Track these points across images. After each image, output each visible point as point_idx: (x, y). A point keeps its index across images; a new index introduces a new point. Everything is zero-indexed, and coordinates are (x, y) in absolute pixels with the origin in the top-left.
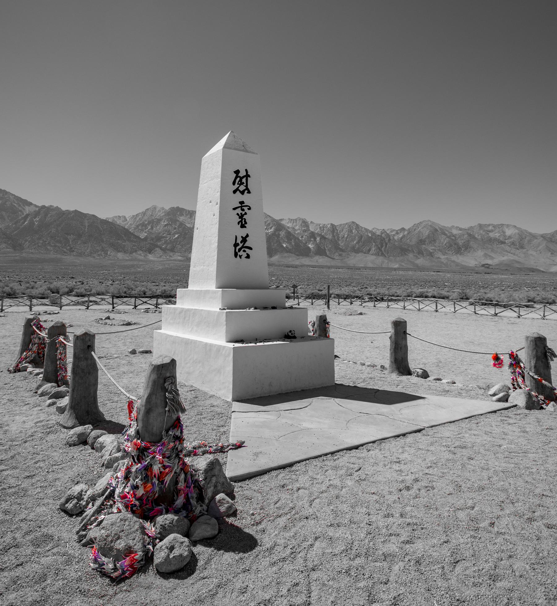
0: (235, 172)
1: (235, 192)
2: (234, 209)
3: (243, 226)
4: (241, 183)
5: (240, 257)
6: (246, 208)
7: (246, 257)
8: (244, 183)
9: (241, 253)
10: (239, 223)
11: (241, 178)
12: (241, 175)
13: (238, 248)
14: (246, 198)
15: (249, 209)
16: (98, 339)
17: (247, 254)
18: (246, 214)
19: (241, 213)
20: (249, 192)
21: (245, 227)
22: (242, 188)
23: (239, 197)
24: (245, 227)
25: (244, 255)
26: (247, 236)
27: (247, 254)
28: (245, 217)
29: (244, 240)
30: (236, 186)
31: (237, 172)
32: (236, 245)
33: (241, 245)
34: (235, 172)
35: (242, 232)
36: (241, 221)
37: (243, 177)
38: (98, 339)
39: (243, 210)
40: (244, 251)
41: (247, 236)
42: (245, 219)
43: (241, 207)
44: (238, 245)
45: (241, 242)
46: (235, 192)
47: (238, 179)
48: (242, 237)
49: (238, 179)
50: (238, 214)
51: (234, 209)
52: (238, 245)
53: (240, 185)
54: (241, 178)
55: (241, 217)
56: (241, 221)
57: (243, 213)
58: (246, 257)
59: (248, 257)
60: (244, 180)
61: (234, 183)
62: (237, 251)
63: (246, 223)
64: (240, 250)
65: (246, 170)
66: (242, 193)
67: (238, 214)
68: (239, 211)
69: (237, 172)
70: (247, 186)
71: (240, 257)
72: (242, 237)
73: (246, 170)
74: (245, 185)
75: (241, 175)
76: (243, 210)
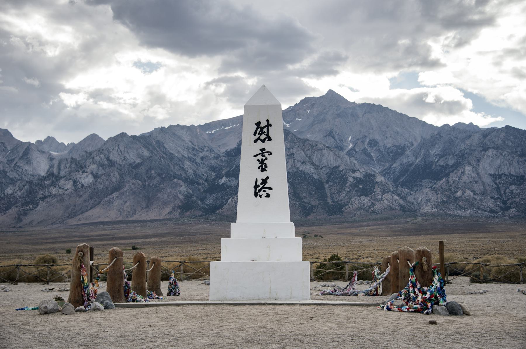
0: (256, 124)
1: (256, 141)
2: (255, 156)
3: (263, 170)
4: (262, 132)
5: (261, 196)
6: (266, 154)
7: (266, 197)
8: (265, 132)
9: (261, 193)
10: (259, 168)
12: (262, 125)
13: (258, 189)
14: (267, 145)
15: (270, 154)
17: (267, 194)
18: (266, 159)
19: (262, 159)
20: (270, 139)
21: (266, 171)
22: (263, 137)
24: (266, 171)
25: (265, 194)
26: (268, 178)
27: (267, 194)
28: (265, 162)
29: (264, 181)
30: (257, 136)
31: (258, 124)
32: (256, 186)
33: (261, 186)
34: (256, 124)
35: (264, 175)
36: (262, 166)
37: (264, 127)
39: (264, 156)
41: (268, 178)
42: (265, 164)
43: (262, 154)
44: (259, 186)
45: (261, 184)
46: (256, 141)
48: (262, 179)
49: (259, 130)
50: (258, 160)
51: (255, 156)
52: (259, 186)
53: (261, 135)
54: (262, 128)
55: (262, 162)
57: (264, 158)
58: (266, 197)
59: (268, 196)
60: (265, 130)
61: (255, 134)
62: (257, 191)
63: (266, 167)
64: (260, 191)
65: (268, 121)
67: (258, 160)
68: (260, 157)
71: (261, 196)
72: (262, 179)
73: (268, 121)
74: (266, 134)
75: (262, 125)
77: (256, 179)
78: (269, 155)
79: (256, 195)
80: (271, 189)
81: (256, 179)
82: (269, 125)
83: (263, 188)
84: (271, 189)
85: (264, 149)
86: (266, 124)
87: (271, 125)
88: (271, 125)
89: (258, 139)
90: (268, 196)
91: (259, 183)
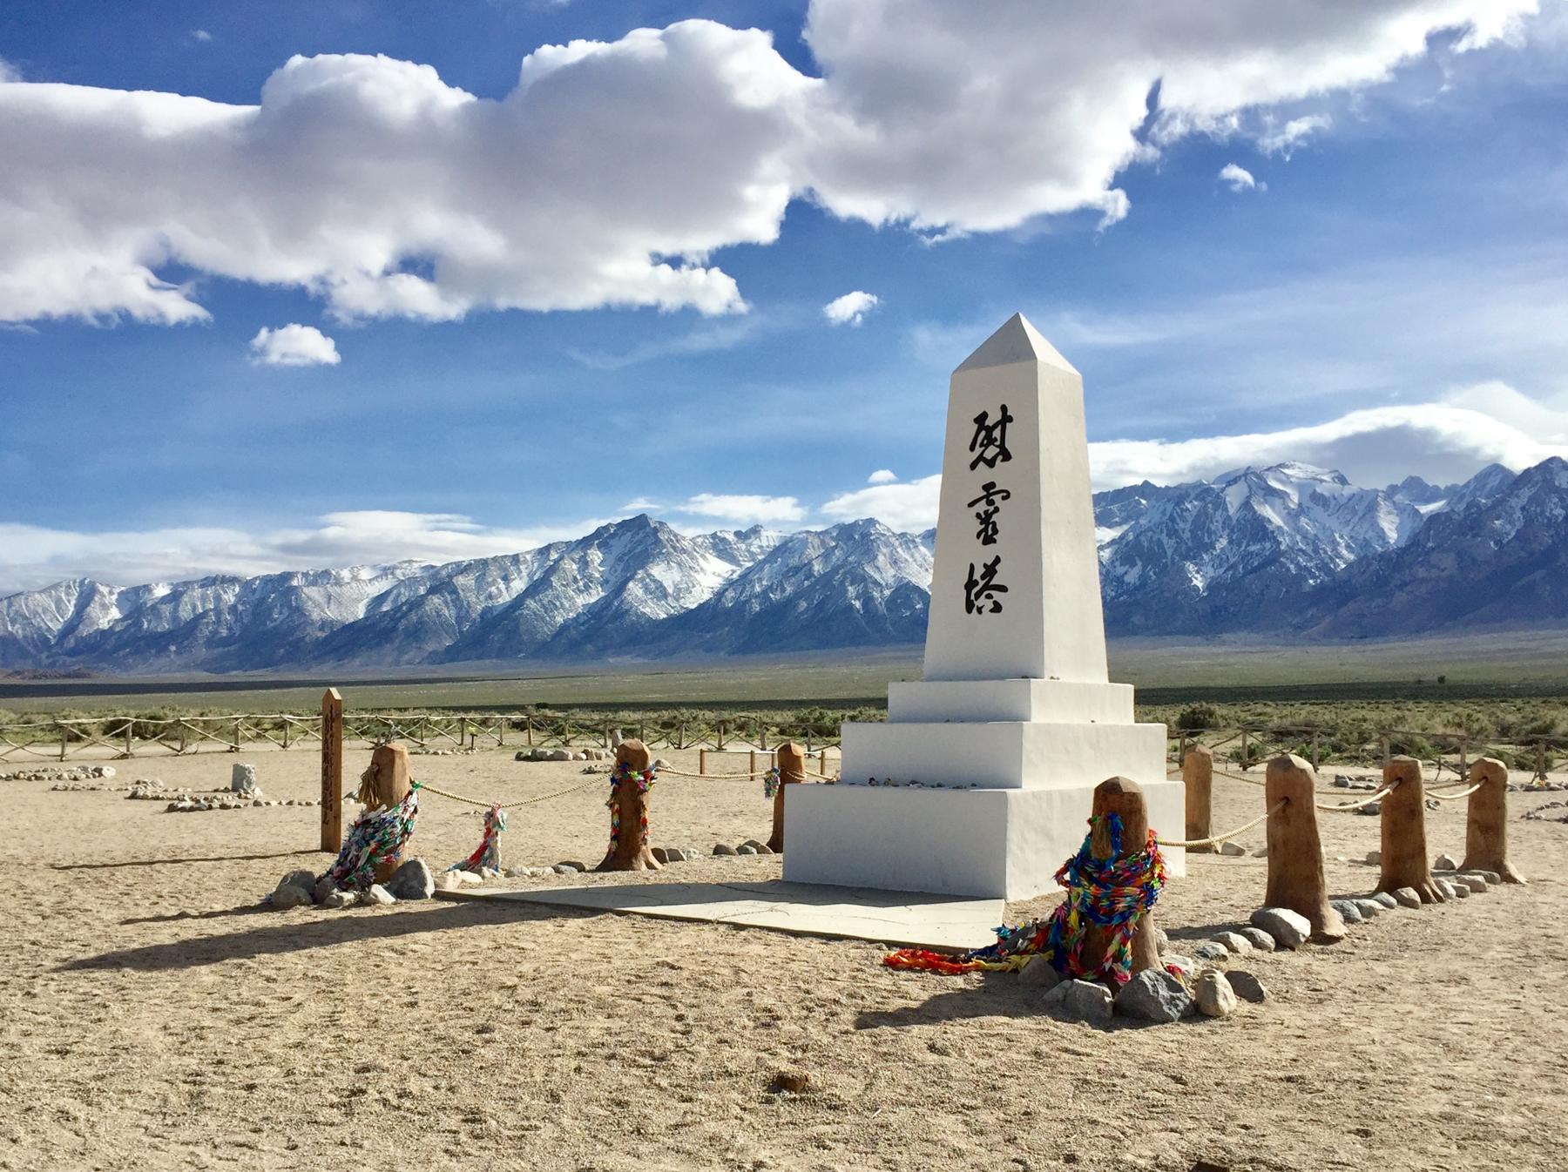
0: (976, 421)
1: (973, 466)
2: (971, 505)
3: (989, 540)
4: (990, 441)
5: (980, 610)
6: (997, 498)
9: (982, 601)
11: (990, 430)
12: (989, 422)
13: (974, 591)
14: (1001, 475)
16: (313, 823)
17: (996, 603)
18: (997, 510)
21: (995, 541)
22: (991, 452)
23: (984, 474)
24: (995, 541)
25: (989, 604)
26: (997, 560)
27: (996, 603)
29: (990, 570)
30: (978, 450)
32: (970, 584)
33: (982, 583)
35: (986, 554)
36: (985, 530)
37: (995, 426)
38: (313, 823)
39: (990, 503)
40: (989, 597)
41: (997, 560)
42: (994, 524)
44: (977, 583)
45: (983, 578)
46: (973, 466)
47: (983, 433)
49: (983, 433)
50: (978, 515)
51: (971, 505)
52: (977, 583)
53: (987, 447)
54: (990, 430)
55: (986, 519)
56: (985, 530)
59: (997, 608)
60: (997, 433)
61: (972, 448)
63: (995, 531)
64: (978, 596)
65: (1004, 408)
66: (991, 463)
67: (978, 515)
68: (982, 507)
69: (982, 418)
70: (1002, 447)
73: (1004, 408)
76: (990, 503)
77: (972, 566)
78: (1004, 498)
79: (969, 610)
80: (1003, 589)
81: (972, 566)
82: (1006, 419)
83: (986, 587)
84: (1003, 589)
85: (992, 485)
86: (999, 416)
87: (1010, 419)
88: (1010, 419)
89: (981, 458)
90: (997, 608)
91: (977, 576)
